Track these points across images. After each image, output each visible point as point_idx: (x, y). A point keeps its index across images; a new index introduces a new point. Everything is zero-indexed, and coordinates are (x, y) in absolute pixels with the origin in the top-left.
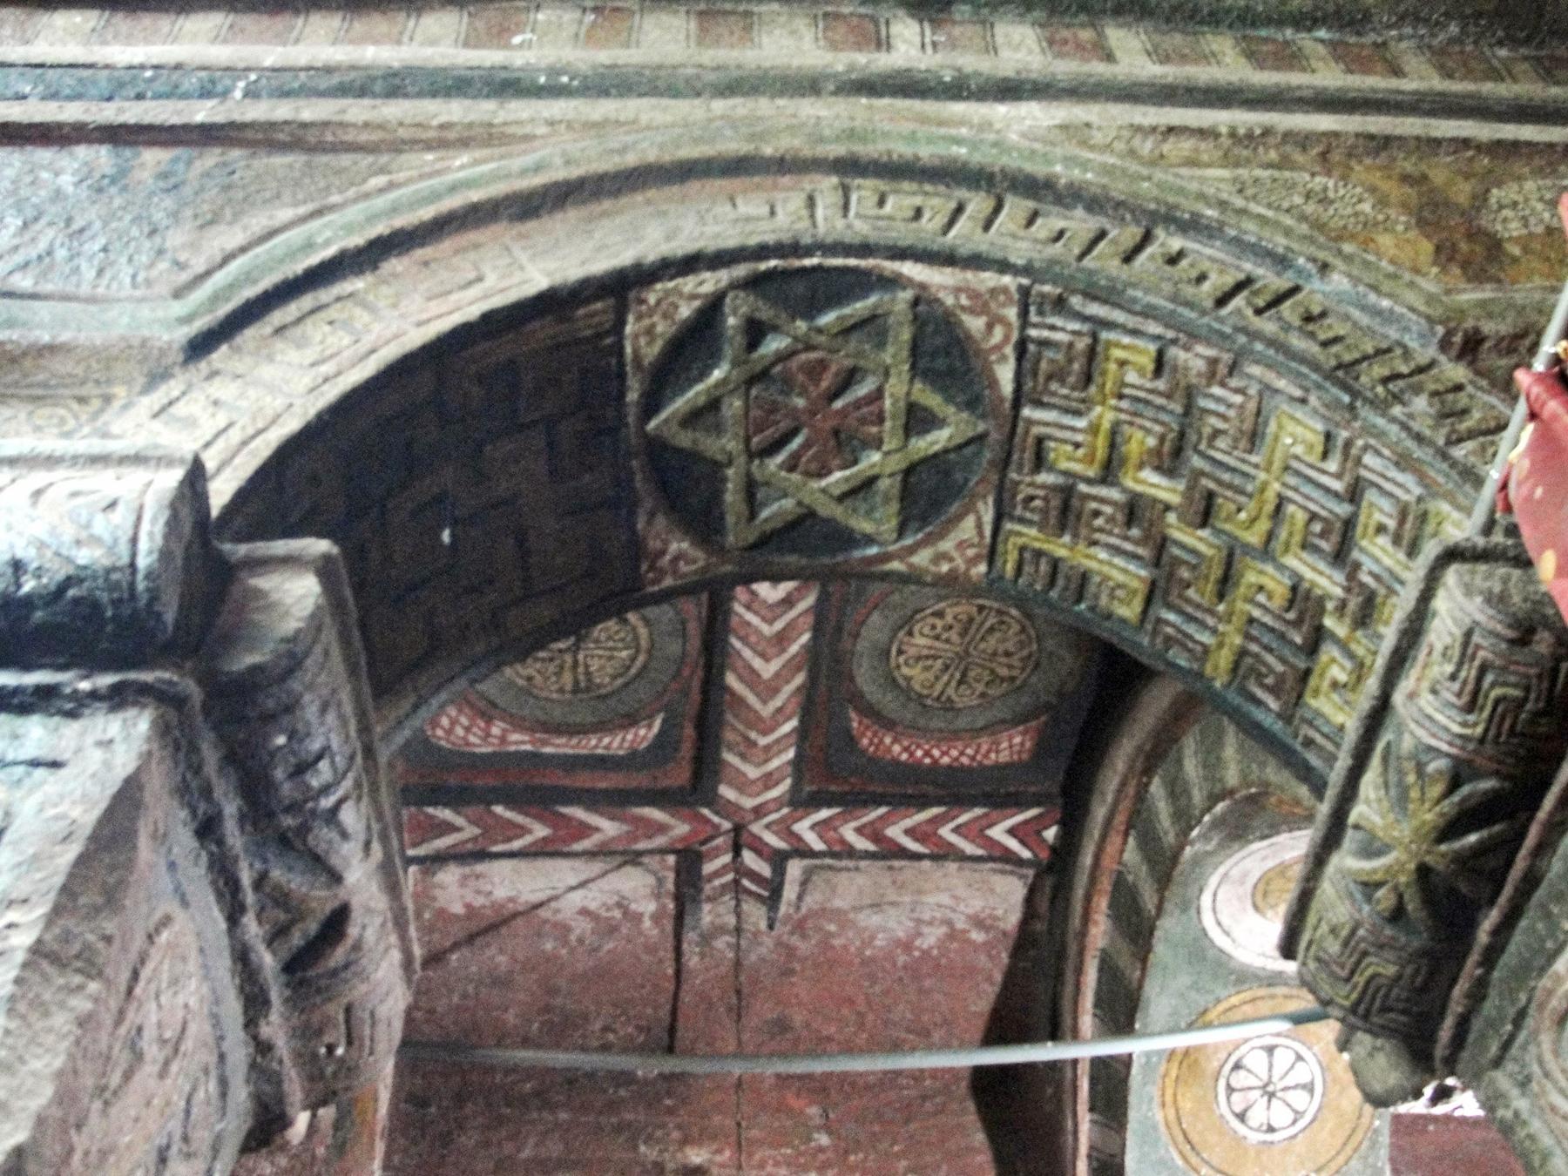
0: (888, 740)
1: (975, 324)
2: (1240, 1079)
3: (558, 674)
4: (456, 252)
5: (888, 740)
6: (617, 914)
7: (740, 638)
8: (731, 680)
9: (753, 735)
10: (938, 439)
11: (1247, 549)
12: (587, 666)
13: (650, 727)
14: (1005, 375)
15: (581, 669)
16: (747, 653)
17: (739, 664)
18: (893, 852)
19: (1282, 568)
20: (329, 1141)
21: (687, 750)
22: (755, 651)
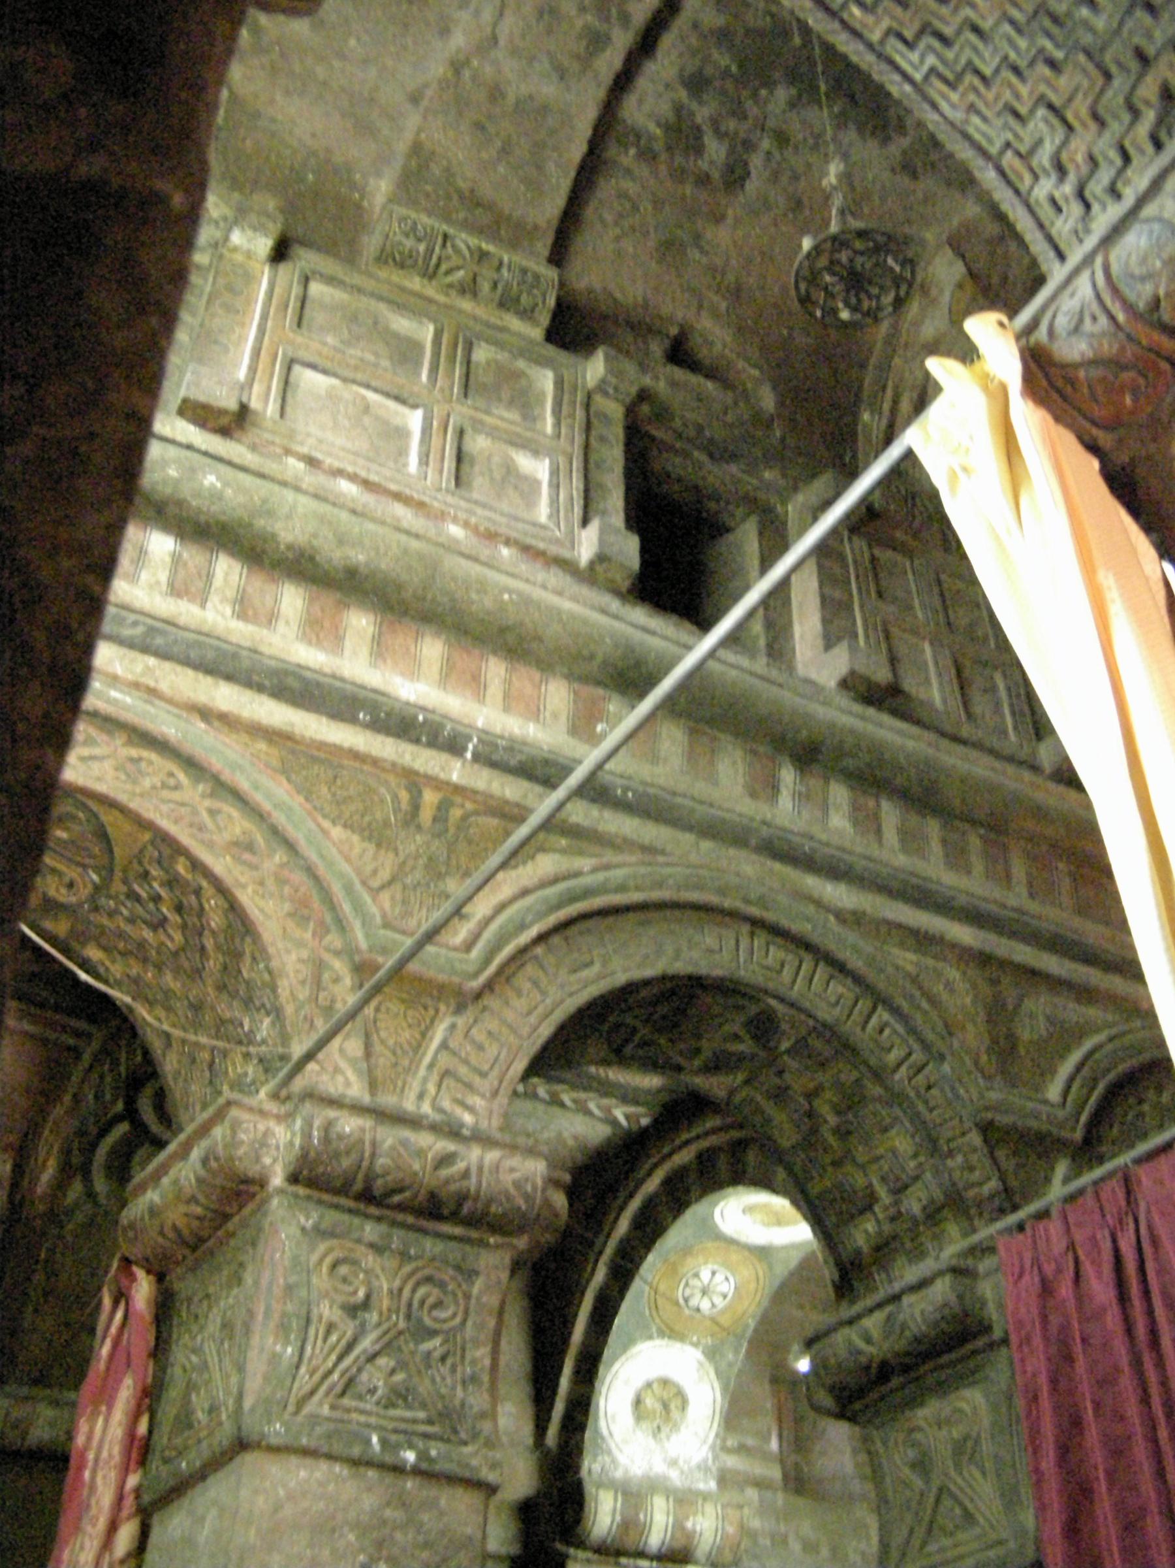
1: (784, 1026)
2: (694, 1282)
4: (581, 933)
10: (741, 1047)
11: (854, 1160)
14: (785, 1045)
18: (556, 1102)
19: (866, 1175)
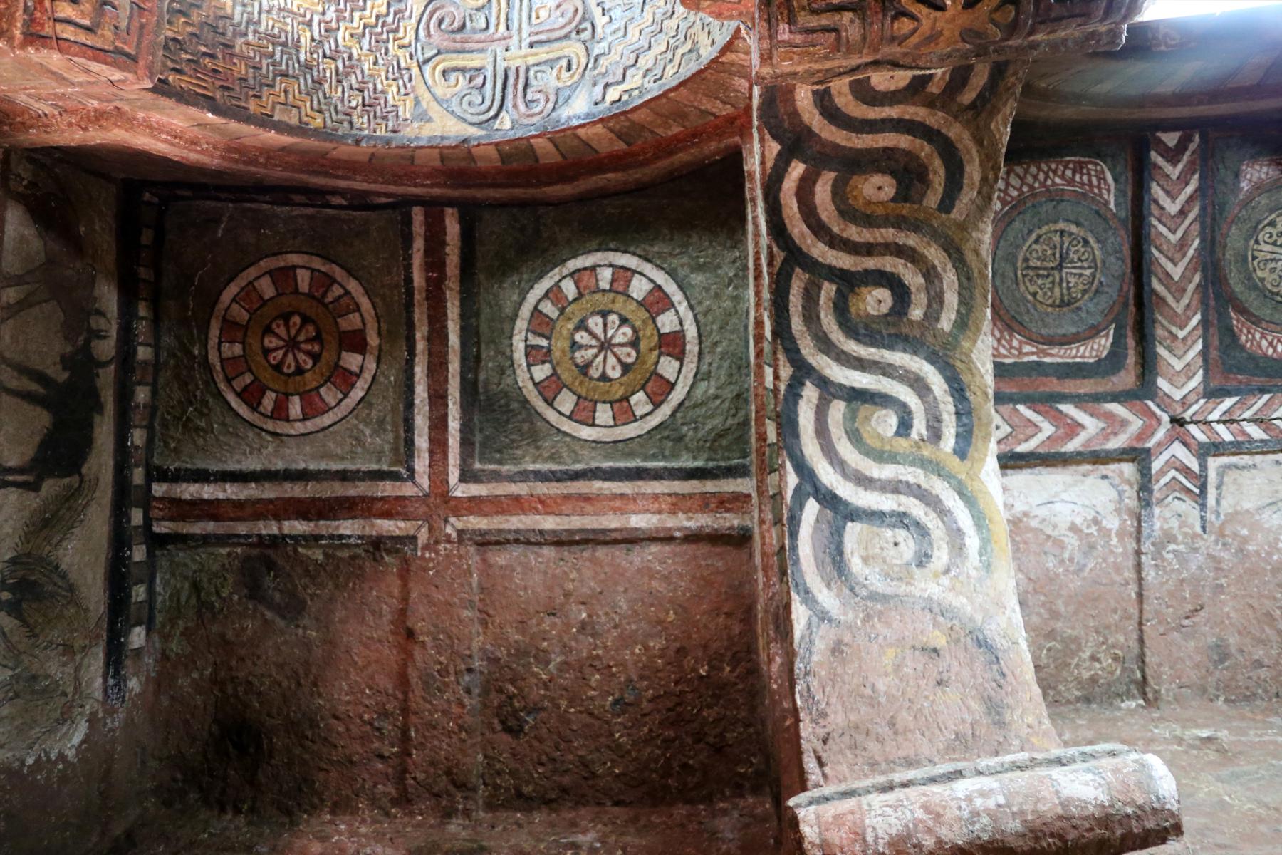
0: (1258, 336)
3: (1051, 290)
5: (1258, 336)
6: (1093, 530)
7: (1156, 248)
8: (1156, 285)
9: (1174, 329)
12: (1068, 282)
13: (1107, 336)
15: (1065, 285)
16: (1163, 260)
17: (1159, 269)
20: (977, 563)
21: (1131, 359)
22: (1167, 257)
